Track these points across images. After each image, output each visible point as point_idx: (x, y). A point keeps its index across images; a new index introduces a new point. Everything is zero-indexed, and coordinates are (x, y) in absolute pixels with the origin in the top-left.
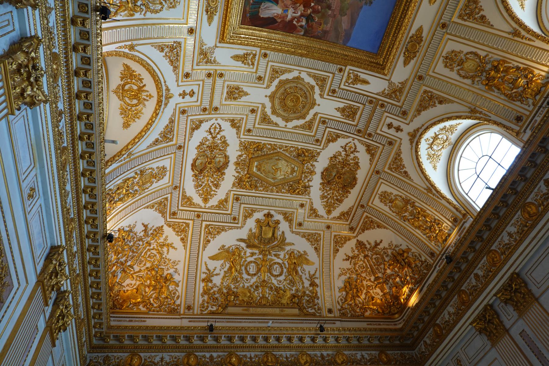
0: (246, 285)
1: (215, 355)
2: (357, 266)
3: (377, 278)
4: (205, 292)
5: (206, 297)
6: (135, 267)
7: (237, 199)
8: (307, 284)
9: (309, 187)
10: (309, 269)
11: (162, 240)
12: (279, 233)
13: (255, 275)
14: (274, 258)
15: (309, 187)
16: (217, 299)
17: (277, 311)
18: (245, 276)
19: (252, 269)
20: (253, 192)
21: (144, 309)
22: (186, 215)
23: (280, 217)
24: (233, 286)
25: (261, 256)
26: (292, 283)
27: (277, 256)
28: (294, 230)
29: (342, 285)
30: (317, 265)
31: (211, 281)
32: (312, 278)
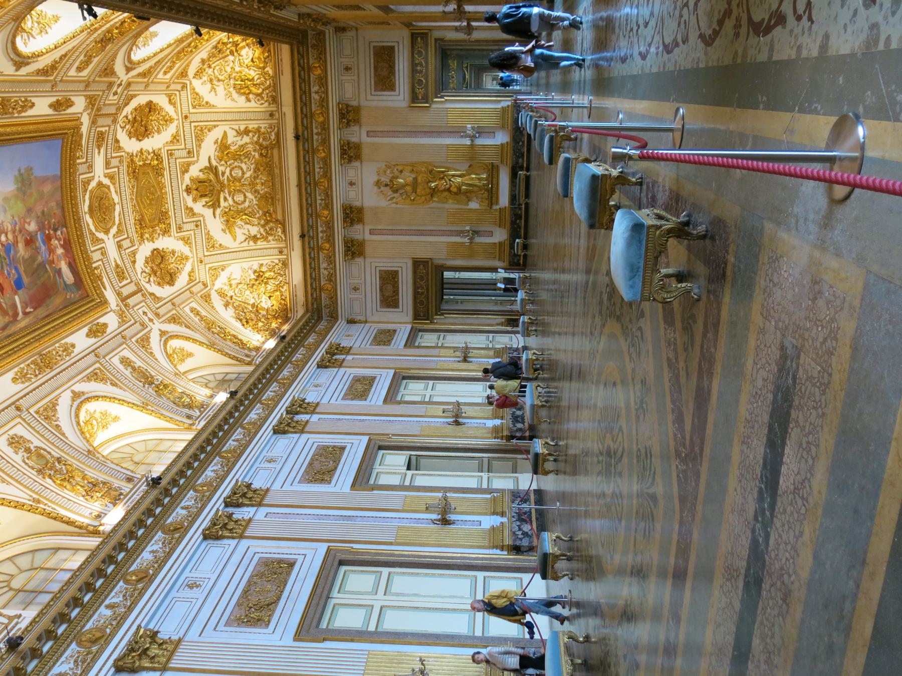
0: (255, 202)
1: (320, 229)
2: (221, 78)
3: (232, 53)
4: (265, 239)
5: (270, 238)
6: (251, 303)
7: (180, 228)
8: (246, 139)
9: (154, 152)
10: (231, 135)
11: (226, 288)
12: (202, 176)
13: (245, 195)
14: (226, 177)
15: (154, 152)
16: (271, 229)
17: (277, 171)
18: (247, 204)
19: (239, 198)
20: (171, 213)
21: (285, 287)
22: (202, 272)
23: (187, 177)
24: (258, 215)
25: (226, 191)
26: (247, 155)
27: (223, 174)
28: (195, 158)
29: (243, 98)
30: (227, 128)
31: (255, 236)
32: (239, 133)
